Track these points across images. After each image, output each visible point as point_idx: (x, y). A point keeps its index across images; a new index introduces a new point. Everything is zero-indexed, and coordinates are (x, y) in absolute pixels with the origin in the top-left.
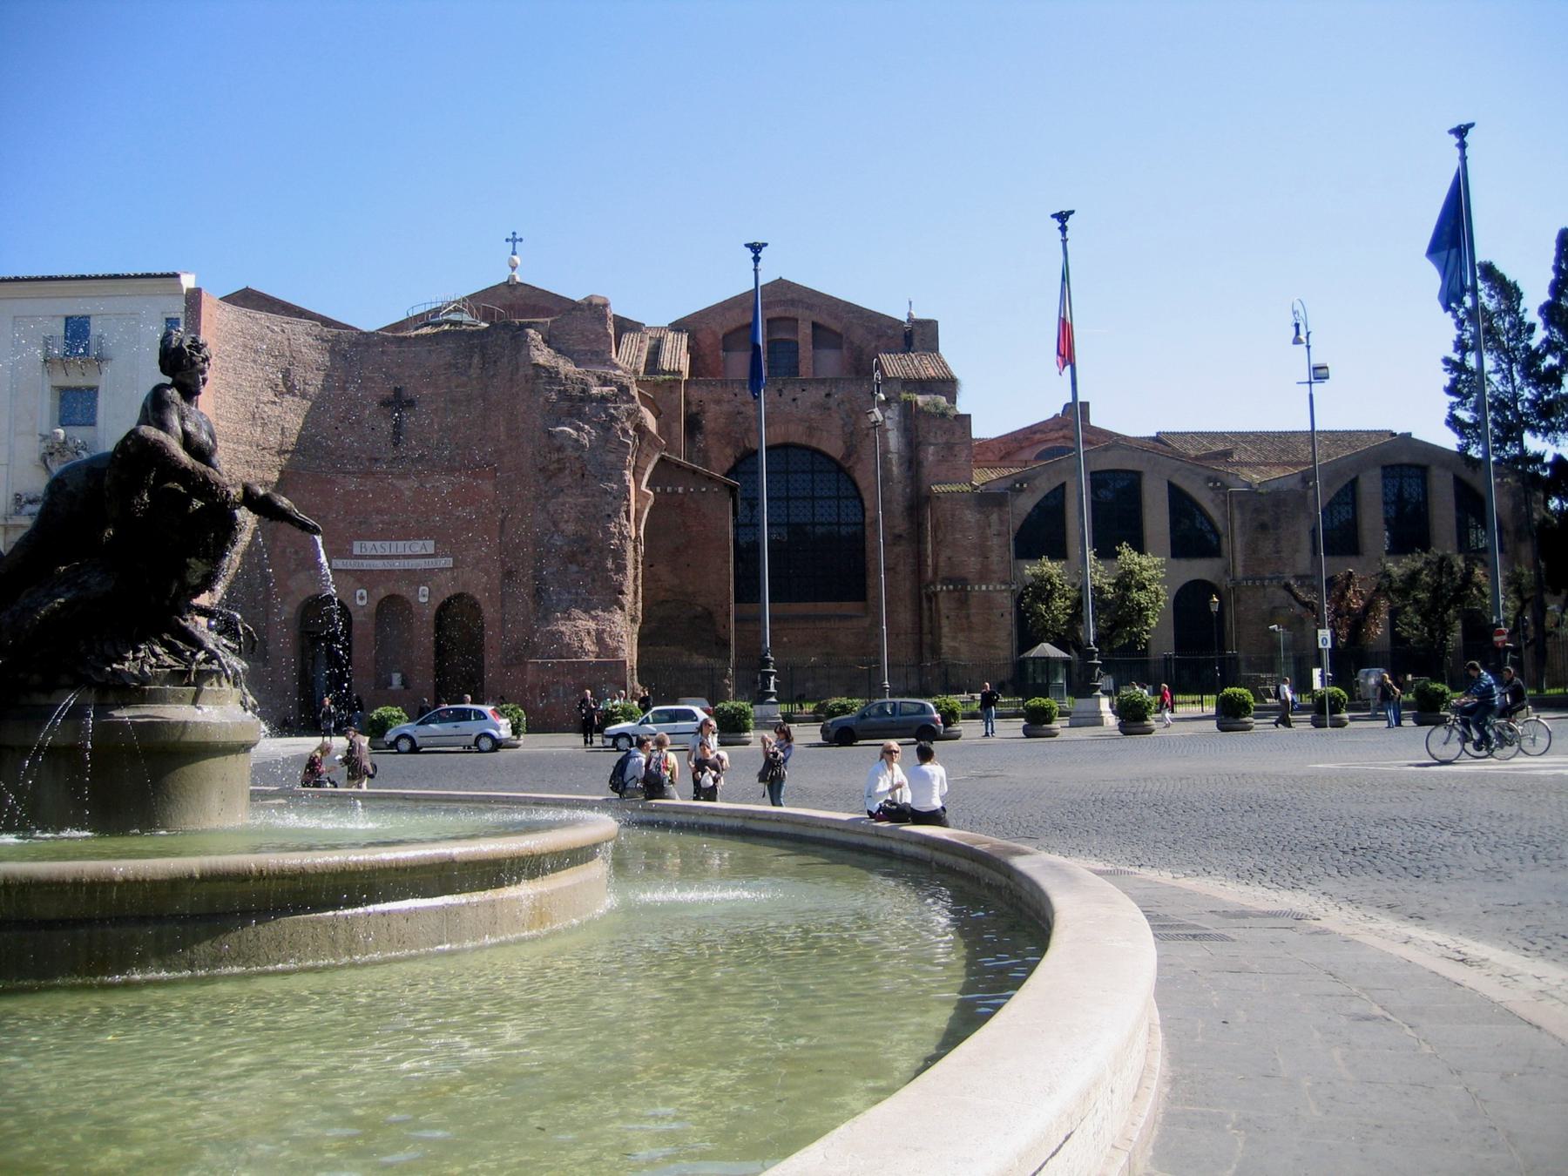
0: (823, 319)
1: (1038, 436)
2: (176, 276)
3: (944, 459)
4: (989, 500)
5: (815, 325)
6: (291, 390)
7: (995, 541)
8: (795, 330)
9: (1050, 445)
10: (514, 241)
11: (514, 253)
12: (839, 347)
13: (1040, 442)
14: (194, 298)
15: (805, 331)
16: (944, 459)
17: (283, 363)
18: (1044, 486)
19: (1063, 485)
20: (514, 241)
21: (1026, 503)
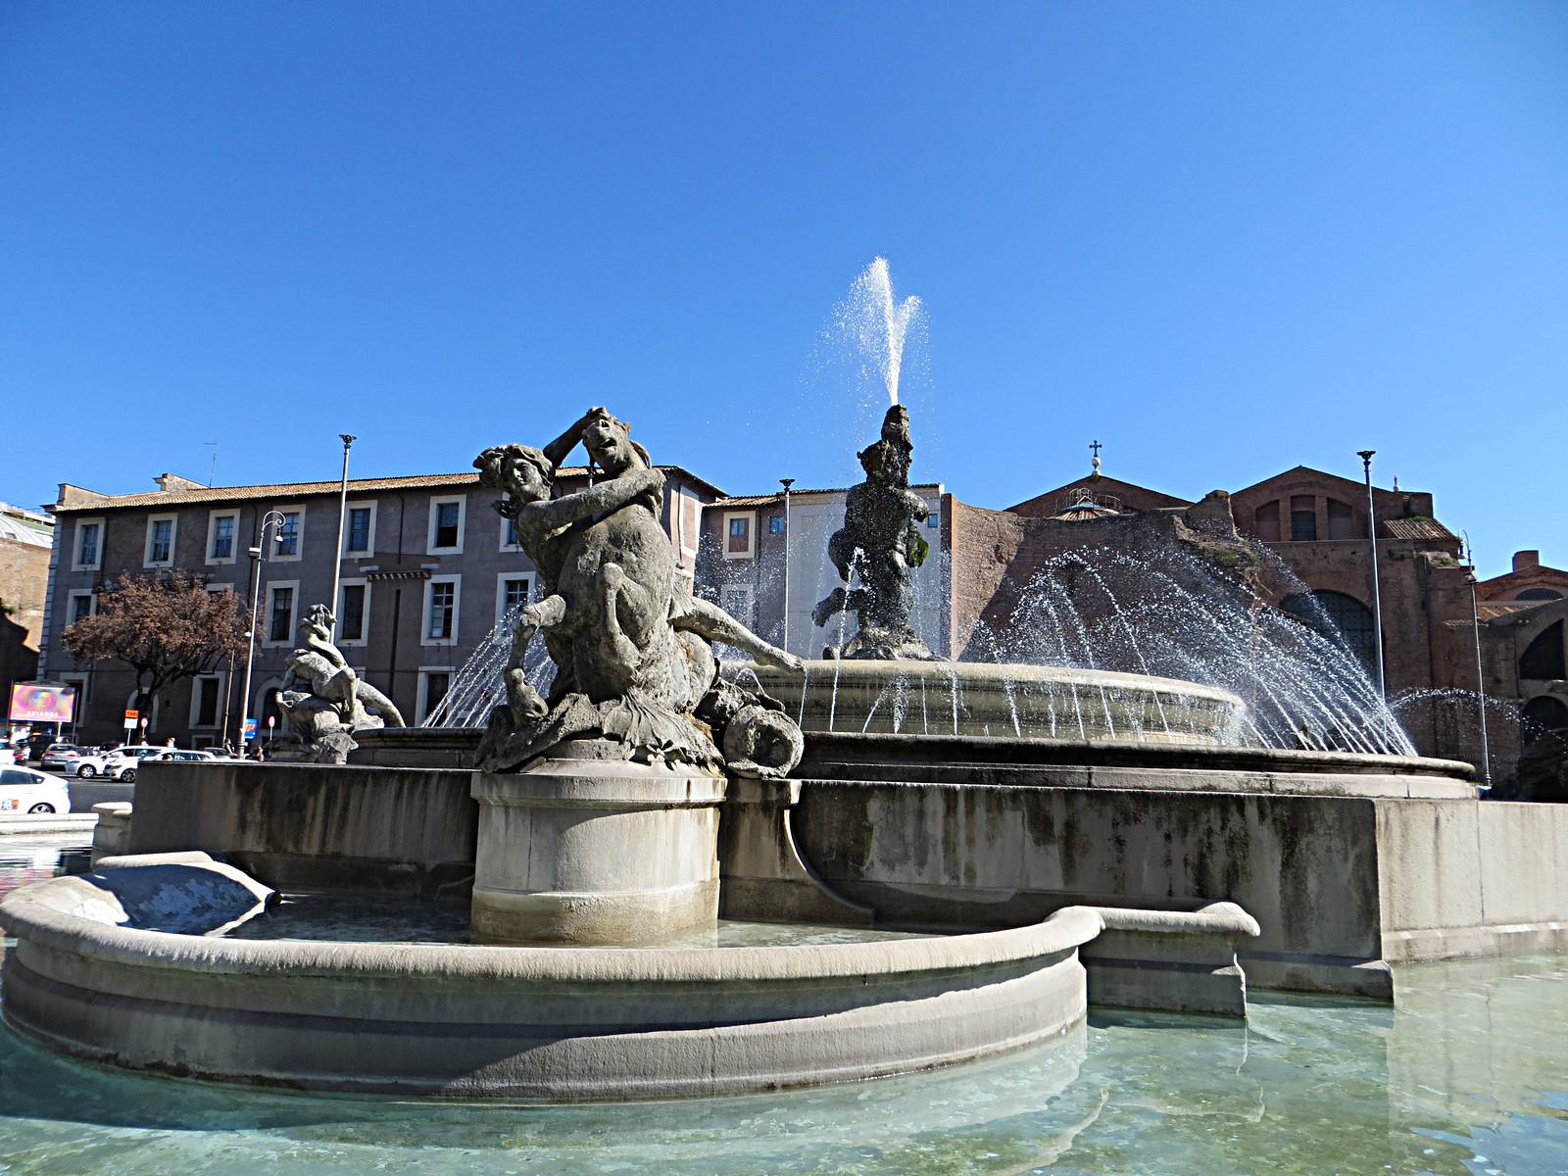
0: (1337, 496)
1: (1519, 581)
2: (937, 486)
3: (1450, 602)
4: (1494, 631)
5: (1329, 499)
6: (1000, 559)
7: (1503, 664)
8: (1313, 504)
9: (1529, 588)
10: (1096, 447)
11: (1096, 456)
12: (1348, 515)
13: (1520, 586)
14: (948, 498)
15: (1321, 504)
16: (1450, 602)
17: (995, 542)
18: (1544, 623)
19: (1561, 622)
20: (1096, 447)
21: (1528, 635)
